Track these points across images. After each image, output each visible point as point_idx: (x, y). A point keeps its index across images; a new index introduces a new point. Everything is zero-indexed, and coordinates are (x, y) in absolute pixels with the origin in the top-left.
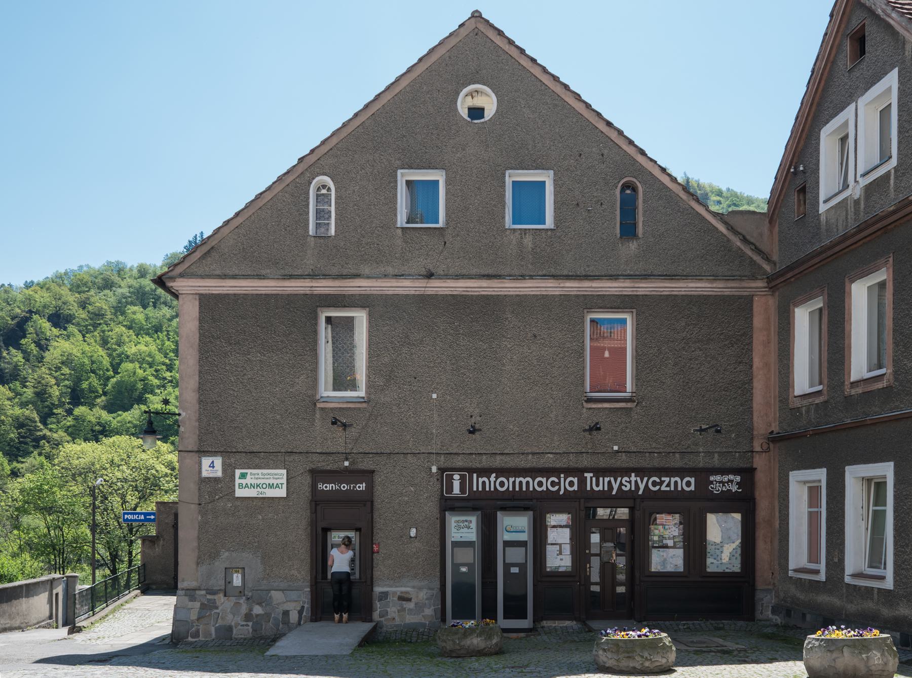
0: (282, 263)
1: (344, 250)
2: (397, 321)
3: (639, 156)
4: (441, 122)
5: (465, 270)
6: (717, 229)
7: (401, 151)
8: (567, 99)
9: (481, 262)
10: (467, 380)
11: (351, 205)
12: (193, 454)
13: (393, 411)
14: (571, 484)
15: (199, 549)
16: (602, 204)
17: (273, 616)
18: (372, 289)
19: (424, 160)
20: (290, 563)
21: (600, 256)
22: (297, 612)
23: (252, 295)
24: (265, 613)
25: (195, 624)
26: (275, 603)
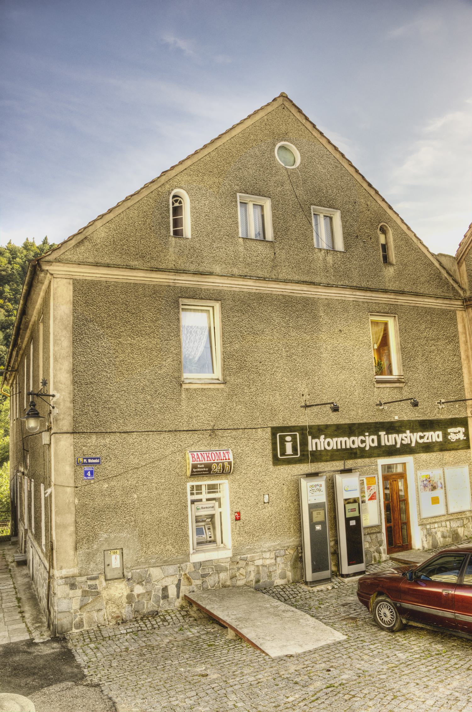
0: (148, 257)
1: (199, 251)
2: (243, 314)
3: (389, 209)
4: (265, 163)
5: (290, 277)
6: (434, 264)
7: (238, 179)
8: (343, 164)
9: (300, 271)
10: (298, 365)
11: (203, 215)
12: (69, 435)
13: (245, 391)
14: (373, 441)
15: (76, 534)
16: (371, 238)
17: (153, 593)
18: (224, 285)
19: (256, 189)
20: (165, 539)
21: (374, 274)
22: (174, 586)
23: (122, 283)
24: (147, 592)
25: (78, 614)
26: (154, 580)
